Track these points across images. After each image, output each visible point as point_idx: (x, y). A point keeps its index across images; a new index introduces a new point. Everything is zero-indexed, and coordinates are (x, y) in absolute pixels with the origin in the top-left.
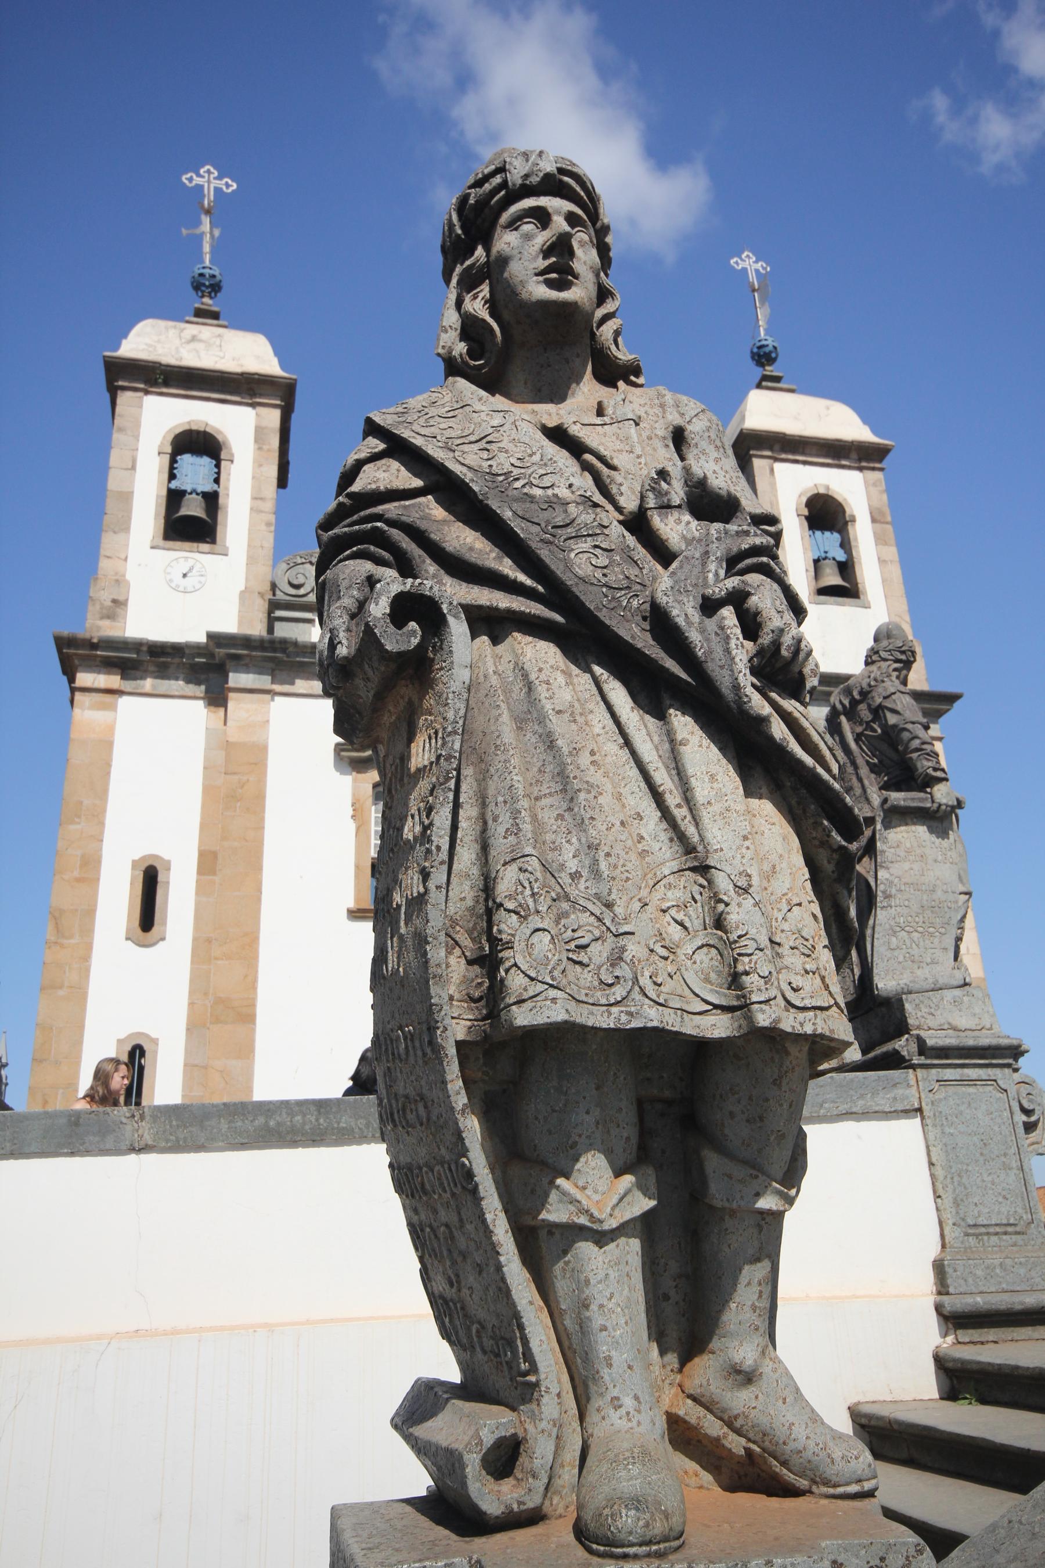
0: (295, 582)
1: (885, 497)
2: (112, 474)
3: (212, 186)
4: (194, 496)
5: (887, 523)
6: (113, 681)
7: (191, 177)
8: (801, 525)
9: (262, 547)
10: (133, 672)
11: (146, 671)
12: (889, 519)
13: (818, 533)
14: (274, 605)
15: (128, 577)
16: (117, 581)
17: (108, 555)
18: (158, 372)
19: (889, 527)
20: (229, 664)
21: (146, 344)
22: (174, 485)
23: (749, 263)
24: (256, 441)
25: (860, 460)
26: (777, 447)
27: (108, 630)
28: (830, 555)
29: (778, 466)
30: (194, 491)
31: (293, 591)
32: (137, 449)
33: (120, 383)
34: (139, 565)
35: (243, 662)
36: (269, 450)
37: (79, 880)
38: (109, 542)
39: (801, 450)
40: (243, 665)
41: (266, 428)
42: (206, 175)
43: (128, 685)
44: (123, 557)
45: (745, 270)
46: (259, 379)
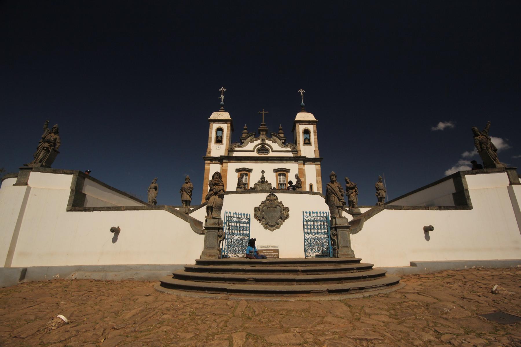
1: (316, 128)
2: (209, 135)
6: (210, 162)
12: (316, 132)
13: (306, 135)
14: (229, 151)
15: (211, 148)
19: (316, 133)
22: (217, 135)
23: (301, 91)
24: (227, 128)
25: (313, 123)
27: (209, 156)
29: (300, 125)
30: (219, 136)
33: (210, 122)
37: (206, 186)
38: (209, 144)
43: (211, 162)
45: (301, 92)
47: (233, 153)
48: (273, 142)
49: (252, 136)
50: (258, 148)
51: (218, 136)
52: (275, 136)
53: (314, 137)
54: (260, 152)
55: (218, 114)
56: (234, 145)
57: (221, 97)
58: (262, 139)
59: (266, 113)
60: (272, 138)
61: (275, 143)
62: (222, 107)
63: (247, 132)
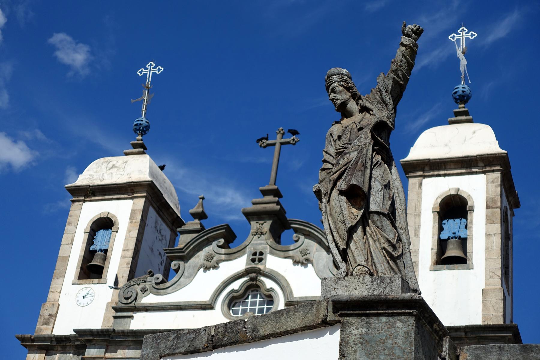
0: (126, 297)
3: (151, 72)
4: (100, 253)
5: (497, 208)
7: (142, 70)
8: (434, 218)
9: (123, 277)
10: (51, 351)
11: (57, 350)
12: (499, 204)
13: (451, 221)
14: (116, 309)
16: (53, 304)
17: (53, 291)
18: (89, 190)
20: (88, 344)
21: (89, 175)
24: (130, 219)
25: (485, 166)
26: (427, 168)
28: (456, 235)
29: (426, 182)
31: (125, 301)
32: (75, 233)
34: (66, 294)
35: (92, 343)
36: (135, 222)
38: (55, 283)
39: (443, 167)
40: (93, 345)
41: (136, 210)
42: (149, 67)
44: (59, 291)
45: (458, 41)
46: (134, 185)
47: (131, 317)
48: (296, 263)
49: (215, 244)
50: (233, 290)
51: (96, 251)
52: (308, 235)
53: (487, 229)
54: (241, 308)
55: (110, 165)
56: (142, 285)
57: (140, 99)
58: (255, 254)
59: (288, 143)
60: (292, 247)
61: (302, 264)
62: (140, 137)
63: (198, 227)
